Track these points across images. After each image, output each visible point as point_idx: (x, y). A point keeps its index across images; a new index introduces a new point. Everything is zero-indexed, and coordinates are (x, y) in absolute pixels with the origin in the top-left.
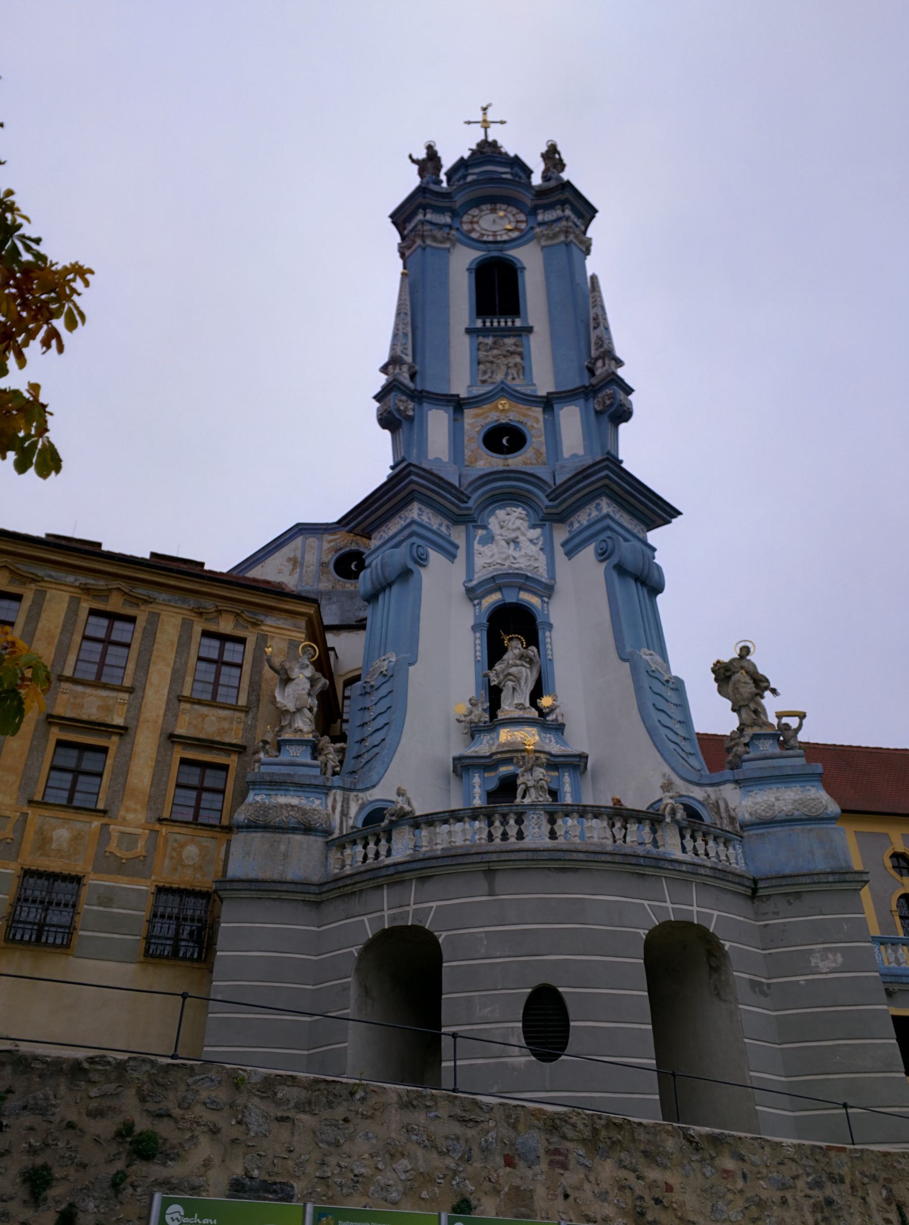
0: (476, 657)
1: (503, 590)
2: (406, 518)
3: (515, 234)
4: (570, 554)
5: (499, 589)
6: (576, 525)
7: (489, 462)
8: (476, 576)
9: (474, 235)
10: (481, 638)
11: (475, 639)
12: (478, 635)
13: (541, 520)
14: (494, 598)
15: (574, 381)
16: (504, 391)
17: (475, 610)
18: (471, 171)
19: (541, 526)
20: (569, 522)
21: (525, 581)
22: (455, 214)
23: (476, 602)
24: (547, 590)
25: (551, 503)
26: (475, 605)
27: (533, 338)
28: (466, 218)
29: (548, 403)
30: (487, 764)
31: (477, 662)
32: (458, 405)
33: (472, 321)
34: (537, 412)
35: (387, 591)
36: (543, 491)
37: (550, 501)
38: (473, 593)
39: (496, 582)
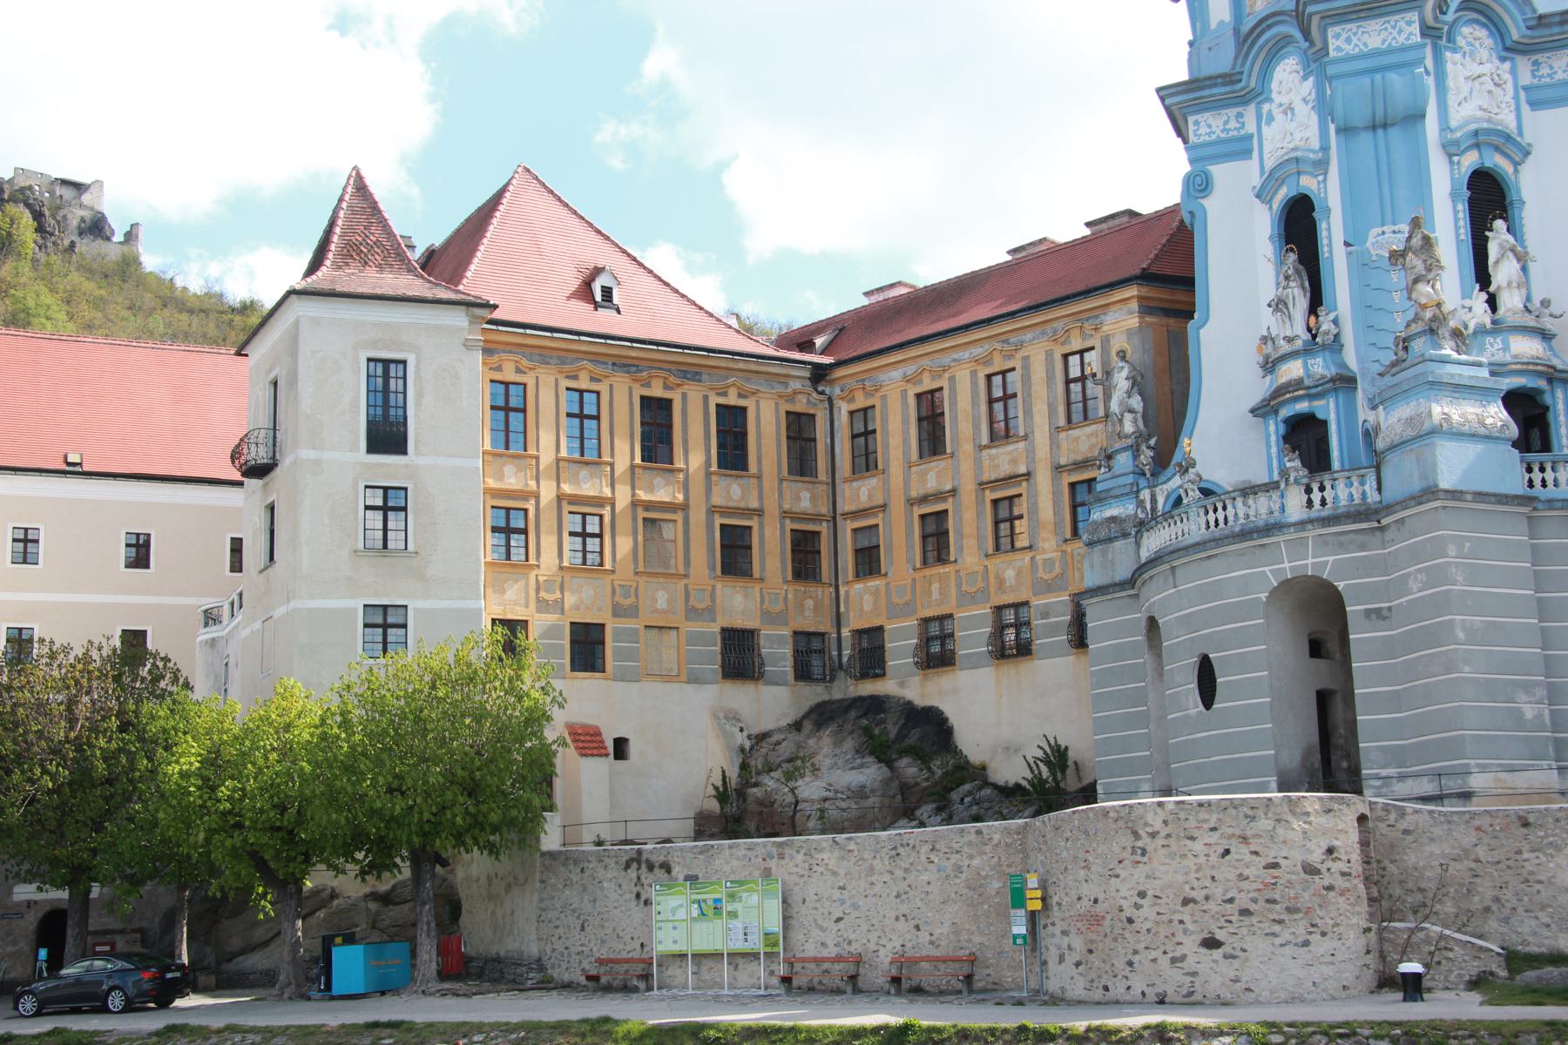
0: (1457, 235)
1: (1483, 149)
2: (1400, 32)
4: (1535, 105)
5: (1477, 146)
6: (1545, 71)
8: (1453, 124)
10: (1463, 208)
11: (1456, 212)
12: (1460, 207)
13: (1507, 49)
14: (1470, 161)
17: (1452, 171)
19: (1512, 60)
20: (1534, 58)
21: (1504, 141)
23: (1456, 159)
25: (1529, 33)
26: (1451, 163)
31: (1459, 242)
35: (1380, 132)
36: (1523, 13)
37: (1529, 28)
38: (1451, 150)
39: (1478, 139)
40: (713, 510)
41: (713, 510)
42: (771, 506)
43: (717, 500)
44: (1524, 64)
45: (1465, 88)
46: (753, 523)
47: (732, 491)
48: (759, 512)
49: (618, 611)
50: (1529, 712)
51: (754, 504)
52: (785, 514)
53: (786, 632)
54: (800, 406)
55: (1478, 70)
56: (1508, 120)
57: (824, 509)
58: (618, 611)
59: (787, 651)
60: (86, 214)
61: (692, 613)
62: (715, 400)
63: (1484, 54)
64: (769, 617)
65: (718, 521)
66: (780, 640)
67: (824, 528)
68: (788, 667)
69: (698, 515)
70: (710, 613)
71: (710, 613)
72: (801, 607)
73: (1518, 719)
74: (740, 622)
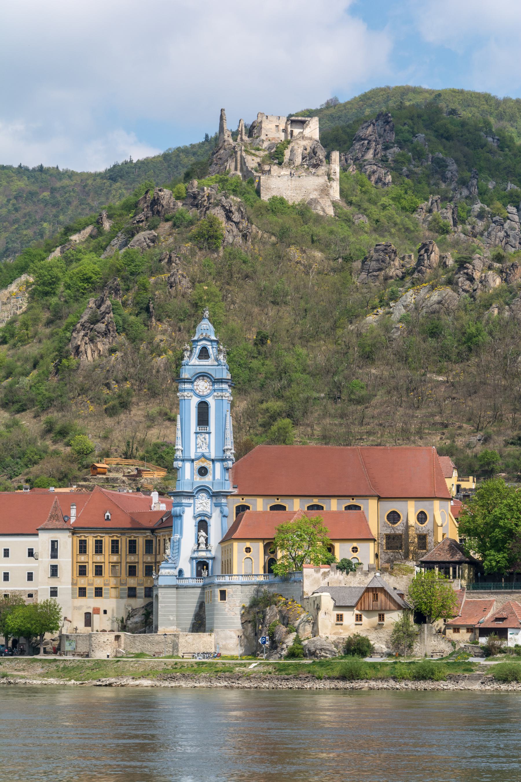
3: (209, 391)
4: (216, 506)
7: (198, 480)
9: (198, 391)
14: (199, 519)
15: (220, 455)
16: (203, 456)
18: (199, 344)
21: (205, 515)
22: (192, 383)
24: (210, 517)
27: (211, 435)
28: (195, 383)
29: (213, 461)
30: (196, 558)
32: (193, 461)
33: (196, 429)
34: (211, 463)
38: (195, 517)
39: (200, 515)
40: (127, 563)
41: (127, 563)
42: (141, 561)
43: (128, 560)
44: (214, 499)
45: (199, 505)
46: (136, 565)
47: (132, 558)
48: (138, 562)
49: (105, 585)
50: (172, 618)
51: (137, 561)
52: (144, 562)
53: (143, 587)
54: (149, 538)
55: (202, 502)
56: (209, 510)
57: (154, 561)
58: (105, 585)
59: (143, 591)
60: (307, 143)
61: (121, 584)
62: (128, 539)
63: (204, 498)
64: (139, 584)
65: (128, 565)
66: (142, 589)
67: (153, 565)
68: (143, 595)
69: (124, 564)
70: (125, 584)
71: (125, 584)
72: (147, 582)
73: (169, 620)
74: (132, 586)
